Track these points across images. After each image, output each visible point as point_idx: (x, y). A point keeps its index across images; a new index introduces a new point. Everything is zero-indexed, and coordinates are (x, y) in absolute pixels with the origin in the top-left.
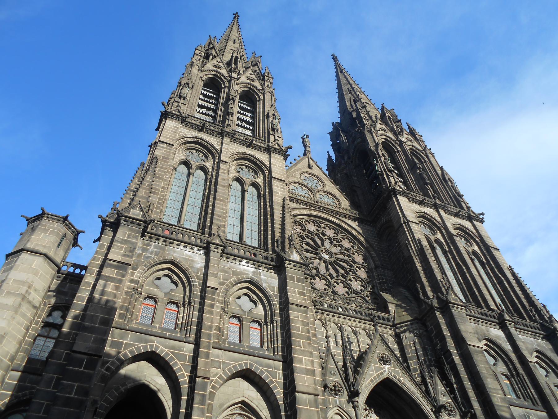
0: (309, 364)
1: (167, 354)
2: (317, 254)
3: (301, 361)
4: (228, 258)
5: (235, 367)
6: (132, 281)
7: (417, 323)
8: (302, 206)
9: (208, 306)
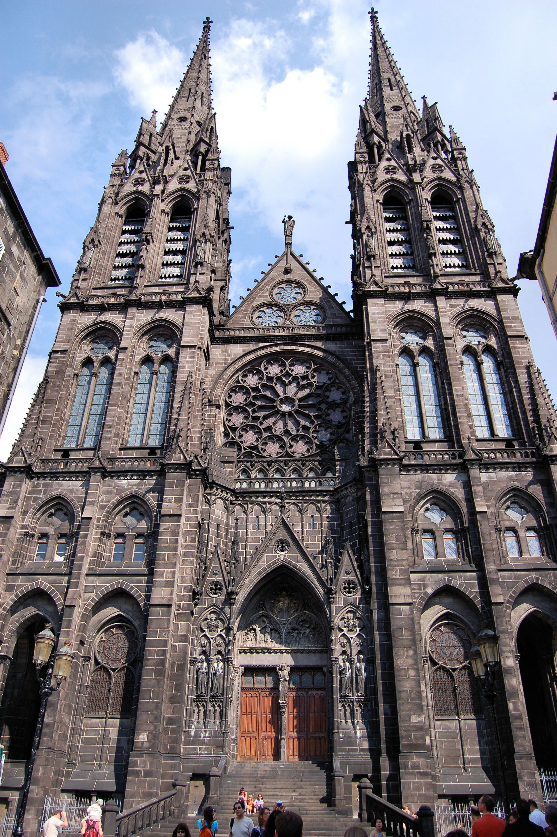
0: (170, 575)
1: (50, 588)
3: (162, 575)
6: (23, 527)
7: (356, 485)
8: (261, 345)
9: (82, 538)
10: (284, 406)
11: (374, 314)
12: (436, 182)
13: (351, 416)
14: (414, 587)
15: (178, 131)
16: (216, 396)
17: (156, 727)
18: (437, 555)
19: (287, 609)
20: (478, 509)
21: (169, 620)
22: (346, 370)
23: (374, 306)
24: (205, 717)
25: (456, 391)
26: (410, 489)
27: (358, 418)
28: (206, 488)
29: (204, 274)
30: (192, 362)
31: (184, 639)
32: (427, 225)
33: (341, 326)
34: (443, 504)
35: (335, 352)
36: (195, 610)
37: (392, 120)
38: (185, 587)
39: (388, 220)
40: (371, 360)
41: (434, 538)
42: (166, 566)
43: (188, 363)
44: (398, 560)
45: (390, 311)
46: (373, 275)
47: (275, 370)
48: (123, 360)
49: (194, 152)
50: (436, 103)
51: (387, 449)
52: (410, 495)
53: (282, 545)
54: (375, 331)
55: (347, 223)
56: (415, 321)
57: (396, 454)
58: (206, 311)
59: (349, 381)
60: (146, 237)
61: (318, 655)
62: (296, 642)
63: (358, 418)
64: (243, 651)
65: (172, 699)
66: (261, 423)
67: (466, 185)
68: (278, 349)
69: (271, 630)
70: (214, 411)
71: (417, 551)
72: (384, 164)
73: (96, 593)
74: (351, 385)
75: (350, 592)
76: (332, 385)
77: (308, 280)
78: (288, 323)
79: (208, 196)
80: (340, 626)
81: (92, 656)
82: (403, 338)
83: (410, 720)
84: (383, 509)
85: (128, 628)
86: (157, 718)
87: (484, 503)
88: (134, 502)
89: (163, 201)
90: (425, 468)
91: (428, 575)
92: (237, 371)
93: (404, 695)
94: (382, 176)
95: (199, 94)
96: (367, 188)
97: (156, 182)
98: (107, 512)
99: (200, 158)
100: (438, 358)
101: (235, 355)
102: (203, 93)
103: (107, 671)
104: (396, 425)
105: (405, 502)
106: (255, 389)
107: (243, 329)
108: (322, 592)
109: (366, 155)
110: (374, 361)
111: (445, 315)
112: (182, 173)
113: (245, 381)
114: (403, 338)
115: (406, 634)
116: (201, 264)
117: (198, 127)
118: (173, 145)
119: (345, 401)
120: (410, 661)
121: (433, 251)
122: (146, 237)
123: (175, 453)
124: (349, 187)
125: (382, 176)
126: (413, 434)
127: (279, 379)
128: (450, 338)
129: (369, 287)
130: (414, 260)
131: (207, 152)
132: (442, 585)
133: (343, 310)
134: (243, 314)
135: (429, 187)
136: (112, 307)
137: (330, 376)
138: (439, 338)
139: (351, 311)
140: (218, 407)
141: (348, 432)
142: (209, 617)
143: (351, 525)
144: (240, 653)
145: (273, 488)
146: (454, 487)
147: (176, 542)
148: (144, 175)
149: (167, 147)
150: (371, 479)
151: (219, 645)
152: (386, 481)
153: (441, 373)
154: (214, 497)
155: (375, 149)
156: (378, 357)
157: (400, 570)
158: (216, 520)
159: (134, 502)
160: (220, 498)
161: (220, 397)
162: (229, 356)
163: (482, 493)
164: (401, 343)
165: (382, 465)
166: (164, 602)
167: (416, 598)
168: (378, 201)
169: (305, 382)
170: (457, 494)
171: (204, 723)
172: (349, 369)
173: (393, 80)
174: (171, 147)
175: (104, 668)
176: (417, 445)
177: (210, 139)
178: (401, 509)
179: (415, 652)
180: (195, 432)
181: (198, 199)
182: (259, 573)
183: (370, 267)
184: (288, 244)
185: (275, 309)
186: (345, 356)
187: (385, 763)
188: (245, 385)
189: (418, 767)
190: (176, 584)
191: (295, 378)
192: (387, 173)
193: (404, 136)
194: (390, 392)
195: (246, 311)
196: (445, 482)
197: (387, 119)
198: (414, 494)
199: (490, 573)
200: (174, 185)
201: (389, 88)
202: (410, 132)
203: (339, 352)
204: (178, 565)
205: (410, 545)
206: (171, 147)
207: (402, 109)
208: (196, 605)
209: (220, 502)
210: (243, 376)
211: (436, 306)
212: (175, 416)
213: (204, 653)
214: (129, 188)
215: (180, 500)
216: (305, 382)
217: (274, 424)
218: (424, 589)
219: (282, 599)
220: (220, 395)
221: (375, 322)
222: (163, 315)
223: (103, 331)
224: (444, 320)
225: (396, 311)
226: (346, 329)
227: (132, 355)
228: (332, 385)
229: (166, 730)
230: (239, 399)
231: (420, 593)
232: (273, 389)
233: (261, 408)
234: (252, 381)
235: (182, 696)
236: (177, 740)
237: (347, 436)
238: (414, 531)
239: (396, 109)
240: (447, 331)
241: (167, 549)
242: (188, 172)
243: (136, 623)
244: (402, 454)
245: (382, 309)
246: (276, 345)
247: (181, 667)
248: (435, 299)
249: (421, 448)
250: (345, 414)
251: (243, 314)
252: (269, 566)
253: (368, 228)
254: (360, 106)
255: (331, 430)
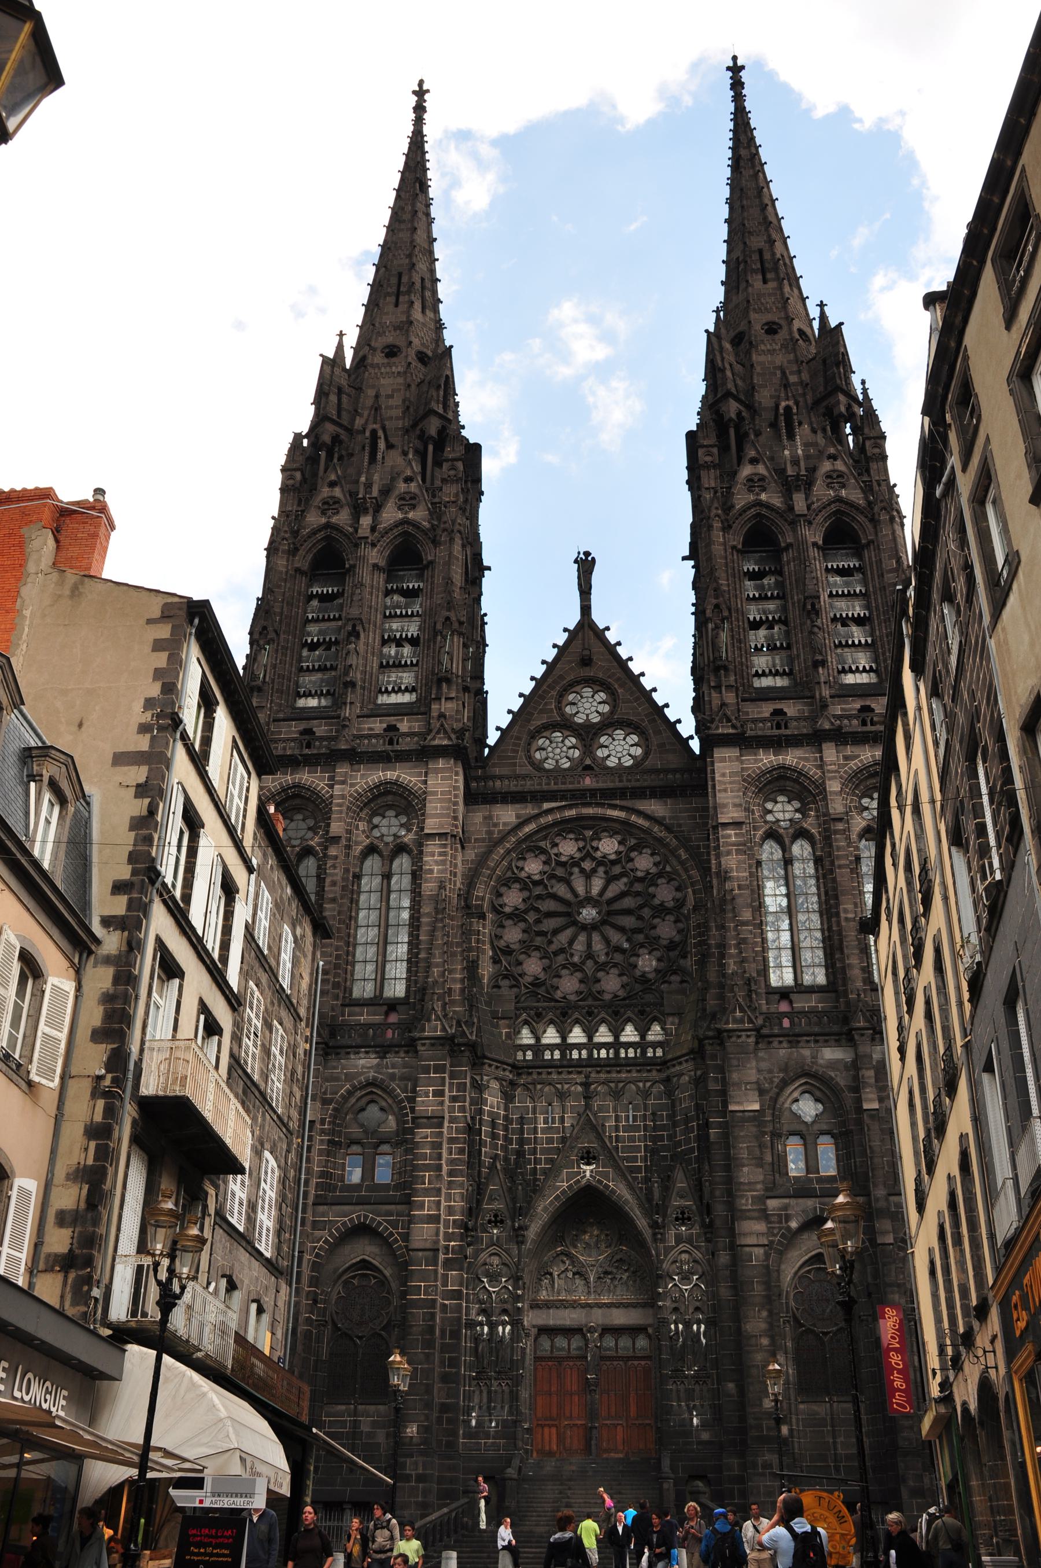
0: (433, 1206)
2: (568, 914)
3: (421, 1206)
4: (338, 1054)
5: (344, 1224)
7: (694, 1059)
8: (546, 806)
10: (584, 912)
11: (723, 775)
12: (833, 508)
13: (689, 930)
14: (773, 1219)
15: (390, 381)
16: (478, 898)
17: (427, 1418)
18: (808, 1172)
19: (597, 1242)
20: (866, 1106)
21: (436, 1271)
22: (682, 852)
23: (723, 760)
24: (490, 1401)
25: (846, 911)
26: (770, 1071)
27: (700, 935)
28: (474, 1065)
29: (452, 698)
30: (443, 863)
31: (457, 1295)
32: (813, 605)
33: (674, 771)
34: (818, 1094)
35: (664, 818)
36: (469, 1251)
37: (762, 358)
38: (454, 1221)
39: (753, 576)
40: (718, 856)
41: (805, 1145)
42: (427, 1192)
43: (437, 863)
44: (750, 1183)
45: (748, 769)
46: (723, 704)
47: (568, 848)
48: (336, 857)
49: (418, 432)
50: (842, 324)
51: (738, 1014)
52: (772, 1082)
53: (588, 1157)
54: (725, 806)
55: (684, 558)
56: (788, 783)
57: (750, 1021)
58: (460, 770)
59: (686, 870)
60: (354, 626)
61: (640, 1310)
62: (609, 1291)
63: (700, 935)
64: (535, 1306)
65: (445, 1378)
66: (550, 942)
67: (884, 517)
68: (573, 812)
70: (477, 925)
71: (780, 1164)
72: (747, 471)
73: (330, 1230)
74: (690, 877)
75: (683, 1224)
76: (660, 875)
77: (619, 679)
78: (588, 762)
79: (452, 540)
82: (770, 812)
83: (761, 1405)
84: (732, 1108)
85: (375, 1277)
86: (428, 1405)
87: (874, 1096)
89: (374, 545)
90: (794, 1038)
91: (793, 1202)
92: (508, 852)
93: (754, 1372)
94: (741, 499)
95: (418, 285)
96: (717, 524)
97: (358, 510)
98: (335, 1109)
99: (431, 448)
100: (822, 849)
101: (504, 824)
102: (423, 279)
103: (351, 1339)
104: (752, 969)
105: (762, 1092)
106: (540, 883)
107: (517, 777)
109: (715, 450)
110: (723, 860)
111: (835, 778)
112: (402, 487)
113: (522, 869)
114: (770, 812)
115: (758, 1290)
116: (448, 681)
117: (419, 365)
118: (384, 429)
119: (680, 903)
120: (763, 1326)
121: (820, 658)
122: (354, 626)
123: (429, 1020)
124: (688, 482)
125: (741, 499)
126: (781, 976)
127: (576, 864)
128: (840, 820)
129: (717, 728)
130: (791, 661)
131: (442, 431)
132: (811, 1216)
133: (678, 734)
134: (515, 745)
135: (820, 518)
136: (310, 762)
137: (657, 858)
138: (825, 815)
139: (691, 737)
140: (482, 916)
141: (685, 957)
143: (687, 1120)
144: (532, 1307)
145: (571, 1059)
146: (834, 1069)
147: (440, 1158)
148: (337, 492)
149: (374, 432)
150: (714, 1057)
151: (504, 1301)
152: (735, 1062)
153: (824, 876)
155: (732, 431)
156: (729, 853)
157: (753, 1197)
158: (490, 1113)
159: (372, 1092)
161: (483, 899)
162: (496, 825)
163: (873, 1081)
164: (766, 822)
165: (730, 1037)
166: (428, 1245)
167: (775, 1235)
168: (734, 547)
169: (617, 870)
170: (838, 1079)
171: (489, 1408)
172: (687, 850)
173: (767, 256)
174: (380, 433)
175: (346, 1334)
176: (784, 994)
177: (446, 407)
178: (756, 1107)
179: (771, 1313)
180: (454, 980)
181: (435, 542)
182: (557, 1198)
183: (718, 688)
184: (586, 609)
185: (567, 733)
186: (680, 826)
188: (523, 875)
189: (771, 1466)
190: (443, 1217)
191: (600, 863)
192: (750, 490)
193: (781, 411)
194: (746, 915)
195: (519, 738)
196: (821, 1062)
197: (754, 357)
198: (776, 1080)
199: (877, 1200)
200: (390, 514)
201: (760, 277)
202: (791, 403)
203: (670, 818)
204: (444, 1191)
205: (768, 1158)
206: (380, 433)
207: (781, 327)
208: (469, 1245)
209: (495, 1085)
210: (519, 859)
211: (821, 758)
212: (422, 955)
213: (483, 1311)
214: (314, 519)
215: (439, 1093)
216: (617, 870)
217: (571, 943)
218: (787, 1221)
219: (589, 1229)
220: (482, 892)
221: (725, 790)
222: (390, 775)
223: (297, 801)
224: (834, 786)
225: (759, 768)
226: (681, 776)
227: (348, 847)
228: (660, 875)
229: (439, 1420)
230: (513, 898)
231: (780, 1229)
232: (568, 883)
233: (550, 915)
234: (533, 867)
235: (458, 1373)
236: (455, 1434)
237: (682, 962)
238: (776, 1135)
239: (772, 329)
240: (837, 806)
241: (427, 1168)
242: (413, 487)
243: (386, 1272)
244: (760, 1021)
245: (736, 766)
246: (570, 807)
247: (456, 1334)
248: (820, 745)
249: (791, 1002)
250: (680, 925)
251: (515, 745)
252: (570, 1187)
253: (717, 606)
254: (707, 331)
255: (657, 954)
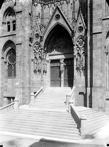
69: (58, 48)
80: (77, 44)
81: (7, 61)
88: (10, 10)
108: (71, 32)
142: (36, 46)
144: (49, 56)
154: (37, 3)
158: (38, 11)
160: (39, 3)
187: (89, 89)
